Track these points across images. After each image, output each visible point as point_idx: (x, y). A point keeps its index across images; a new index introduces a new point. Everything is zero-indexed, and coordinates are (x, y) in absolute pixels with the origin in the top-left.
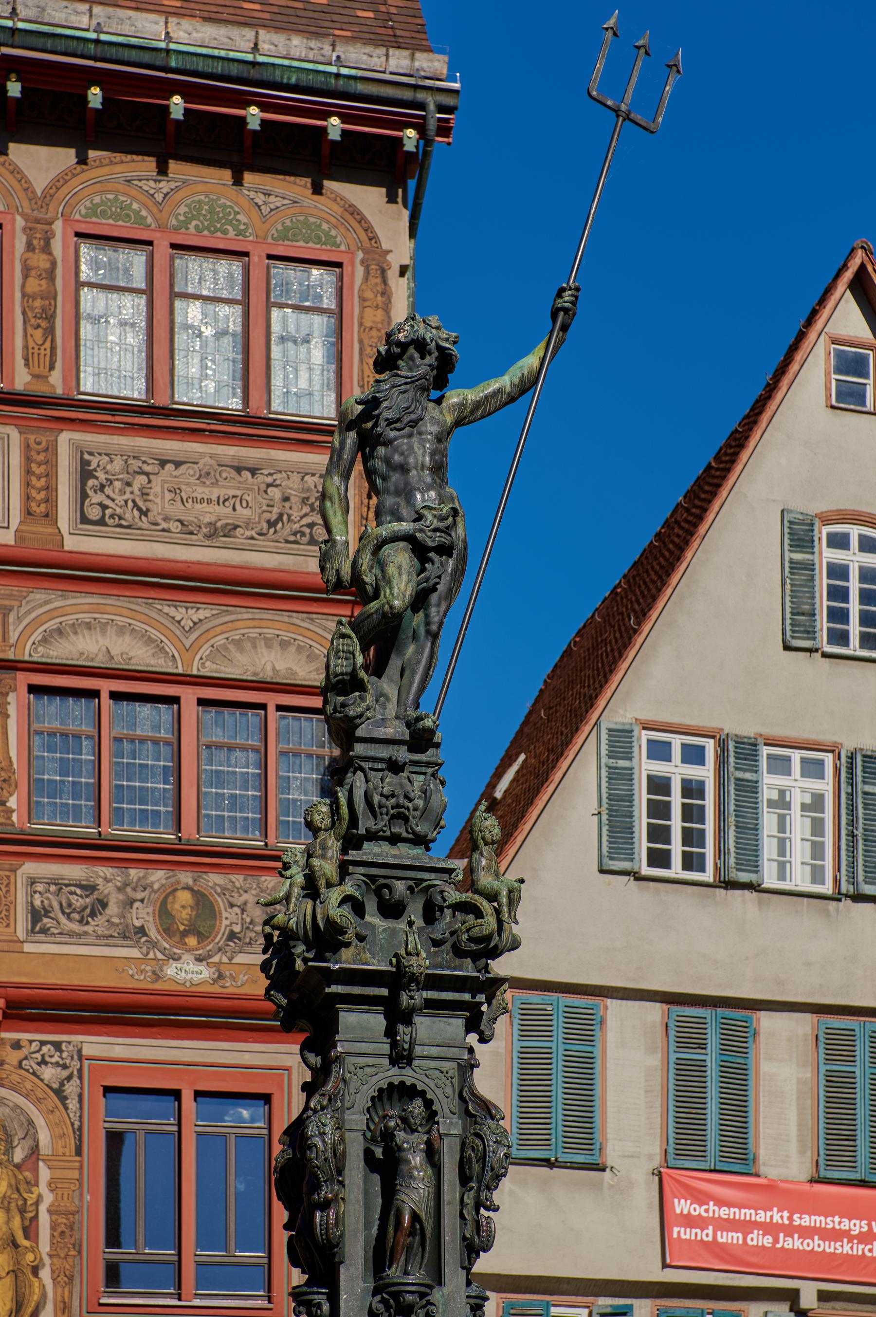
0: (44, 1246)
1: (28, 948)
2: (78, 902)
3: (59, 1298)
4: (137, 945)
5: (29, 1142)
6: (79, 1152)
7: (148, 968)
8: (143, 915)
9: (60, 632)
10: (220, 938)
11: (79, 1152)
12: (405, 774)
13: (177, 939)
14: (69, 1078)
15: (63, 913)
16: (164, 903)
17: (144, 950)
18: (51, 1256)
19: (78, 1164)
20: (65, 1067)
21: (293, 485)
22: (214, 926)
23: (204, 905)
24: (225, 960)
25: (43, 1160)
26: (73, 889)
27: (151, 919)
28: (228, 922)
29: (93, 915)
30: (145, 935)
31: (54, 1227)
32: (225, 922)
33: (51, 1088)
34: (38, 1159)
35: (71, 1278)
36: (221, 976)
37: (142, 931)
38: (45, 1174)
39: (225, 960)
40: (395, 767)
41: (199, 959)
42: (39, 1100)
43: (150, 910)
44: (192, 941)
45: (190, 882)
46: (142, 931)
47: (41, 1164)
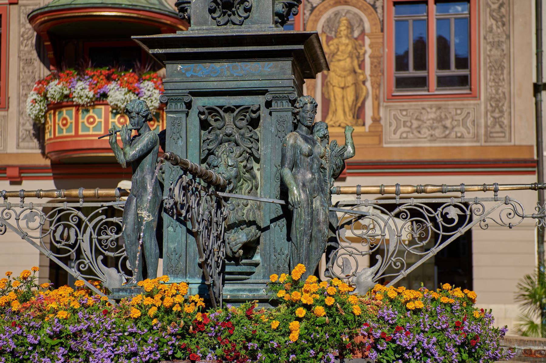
0: (368, 71)
3: (374, 94)
5: (361, 28)
11: (382, 30)
18: (371, 76)
19: (381, 36)
25: (367, 36)
31: (372, 63)
34: (364, 35)
35: (379, 85)
38: (367, 41)
47: (366, 37)
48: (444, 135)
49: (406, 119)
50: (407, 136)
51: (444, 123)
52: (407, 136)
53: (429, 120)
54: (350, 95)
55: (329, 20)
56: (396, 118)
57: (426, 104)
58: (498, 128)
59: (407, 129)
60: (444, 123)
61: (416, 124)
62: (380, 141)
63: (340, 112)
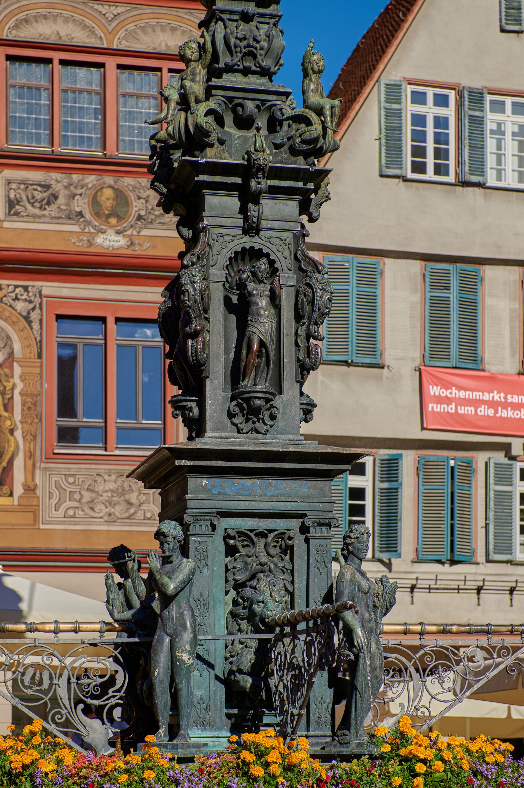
0: (18, 416)
1: (6, 225)
2: (39, 196)
3: (27, 449)
4: (77, 223)
5: (7, 350)
6: (40, 356)
7: (85, 238)
8: (80, 204)
10: (132, 219)
11: (40, 356)
12: (254, 23)
13: (104, 219)
14: (34, 309)
15: (29, 202)
16: (95, 196)
17: (82, 226)
18: (22, 423)
19: (39, 364)
20: (30, 302)
22: (127, 211)
23: (121, 198)
24: (135, 233)
25: (17, 361)
26: (35, 187)
27: (86, 206)
28: (137, 209)
29: (49, 203)
30: (83, 216)
31: (23, 404)
32: (135, 209)
33: (21, 315)
34: (13, 361)
35: (35, 437)
36: (132, 244)
38: (17, 370)
39: (135, 233)
40: (246, 18)
41: (118, 233)
42: (14, 323)
43: (86, 201)
44: (113, 221)
45: (112, 183)
46: (80, 214)
47: (15, 364)
48: (127, 515)
49: (73, 488)
50: (75, 513)
51: (127, 497)
52: (75, 513)
53: (106, 491)
56: (58, 487)
59: (75, 504)
60: (127, 497)
61: (87, 496)
62: (36, 520)
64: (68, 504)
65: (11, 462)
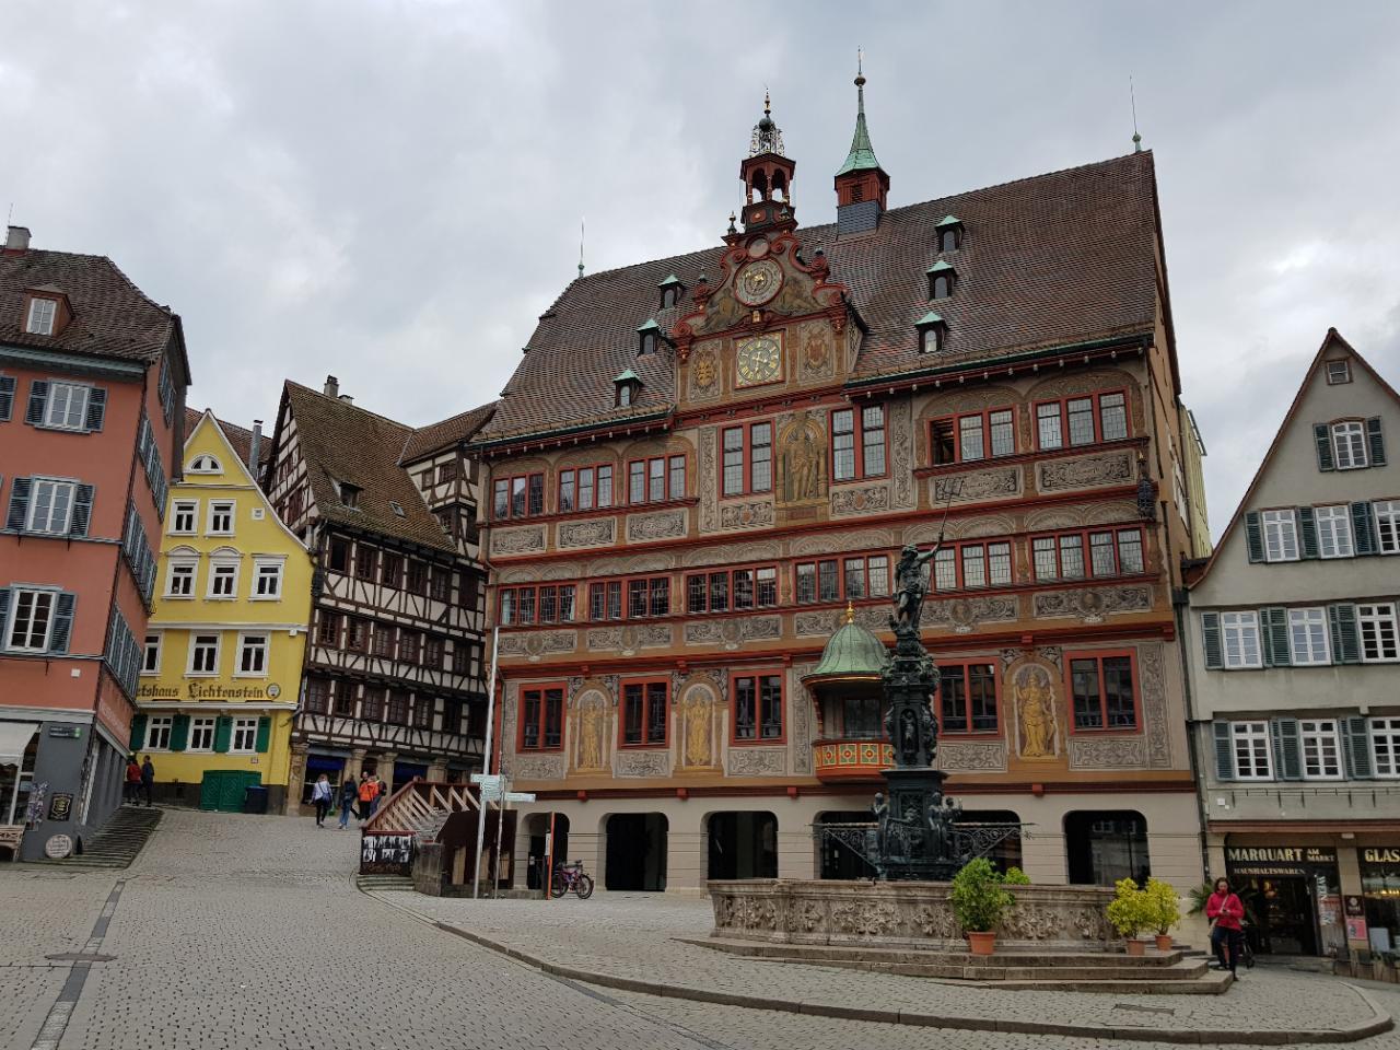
8: (1075, 604)
9: (1040, 520)
21: (1114, 461)
37: (1076, 609)
44: (1093, 610)
46: (1076, 609)
54: (1041, 730)
55: (1020, 674)
57: (1101, 738)
58: (1160, 757)
61: (1095, 753)
63: (1034, 745)
64: (1084, 757)
65: (1052, 738)
